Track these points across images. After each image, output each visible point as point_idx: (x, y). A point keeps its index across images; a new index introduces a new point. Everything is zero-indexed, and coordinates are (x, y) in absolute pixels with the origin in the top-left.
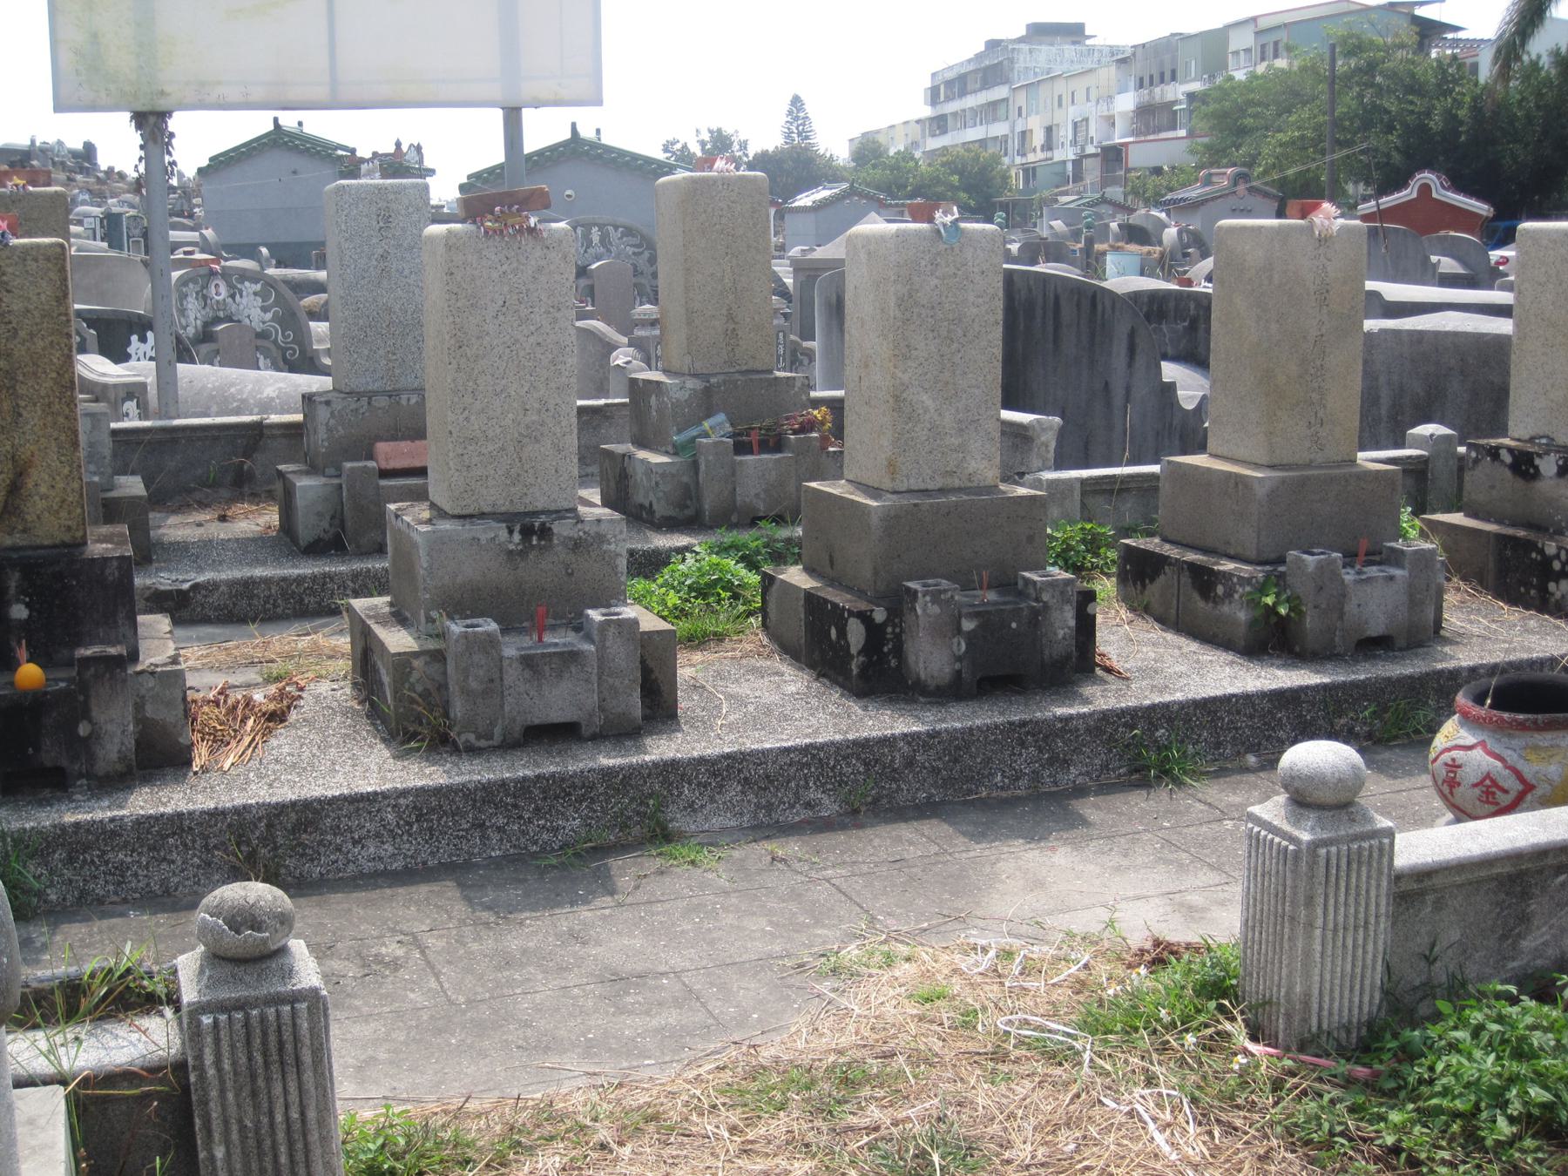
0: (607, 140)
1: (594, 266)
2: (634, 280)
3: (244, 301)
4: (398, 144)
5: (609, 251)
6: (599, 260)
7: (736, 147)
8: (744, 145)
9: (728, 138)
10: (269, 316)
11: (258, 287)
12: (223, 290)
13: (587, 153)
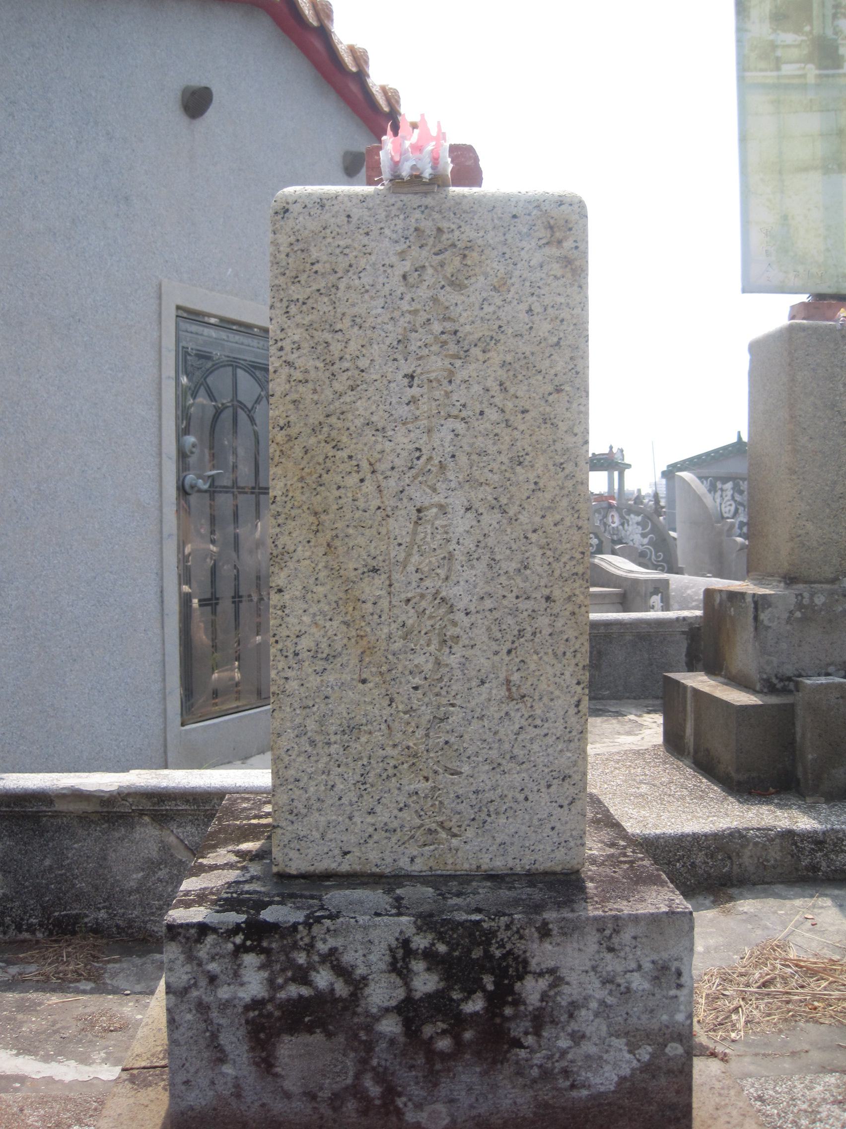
3: (630, 528)
4: (611, 448)
10: (646, 541)
11: (639, 519)
12: (617, 519)
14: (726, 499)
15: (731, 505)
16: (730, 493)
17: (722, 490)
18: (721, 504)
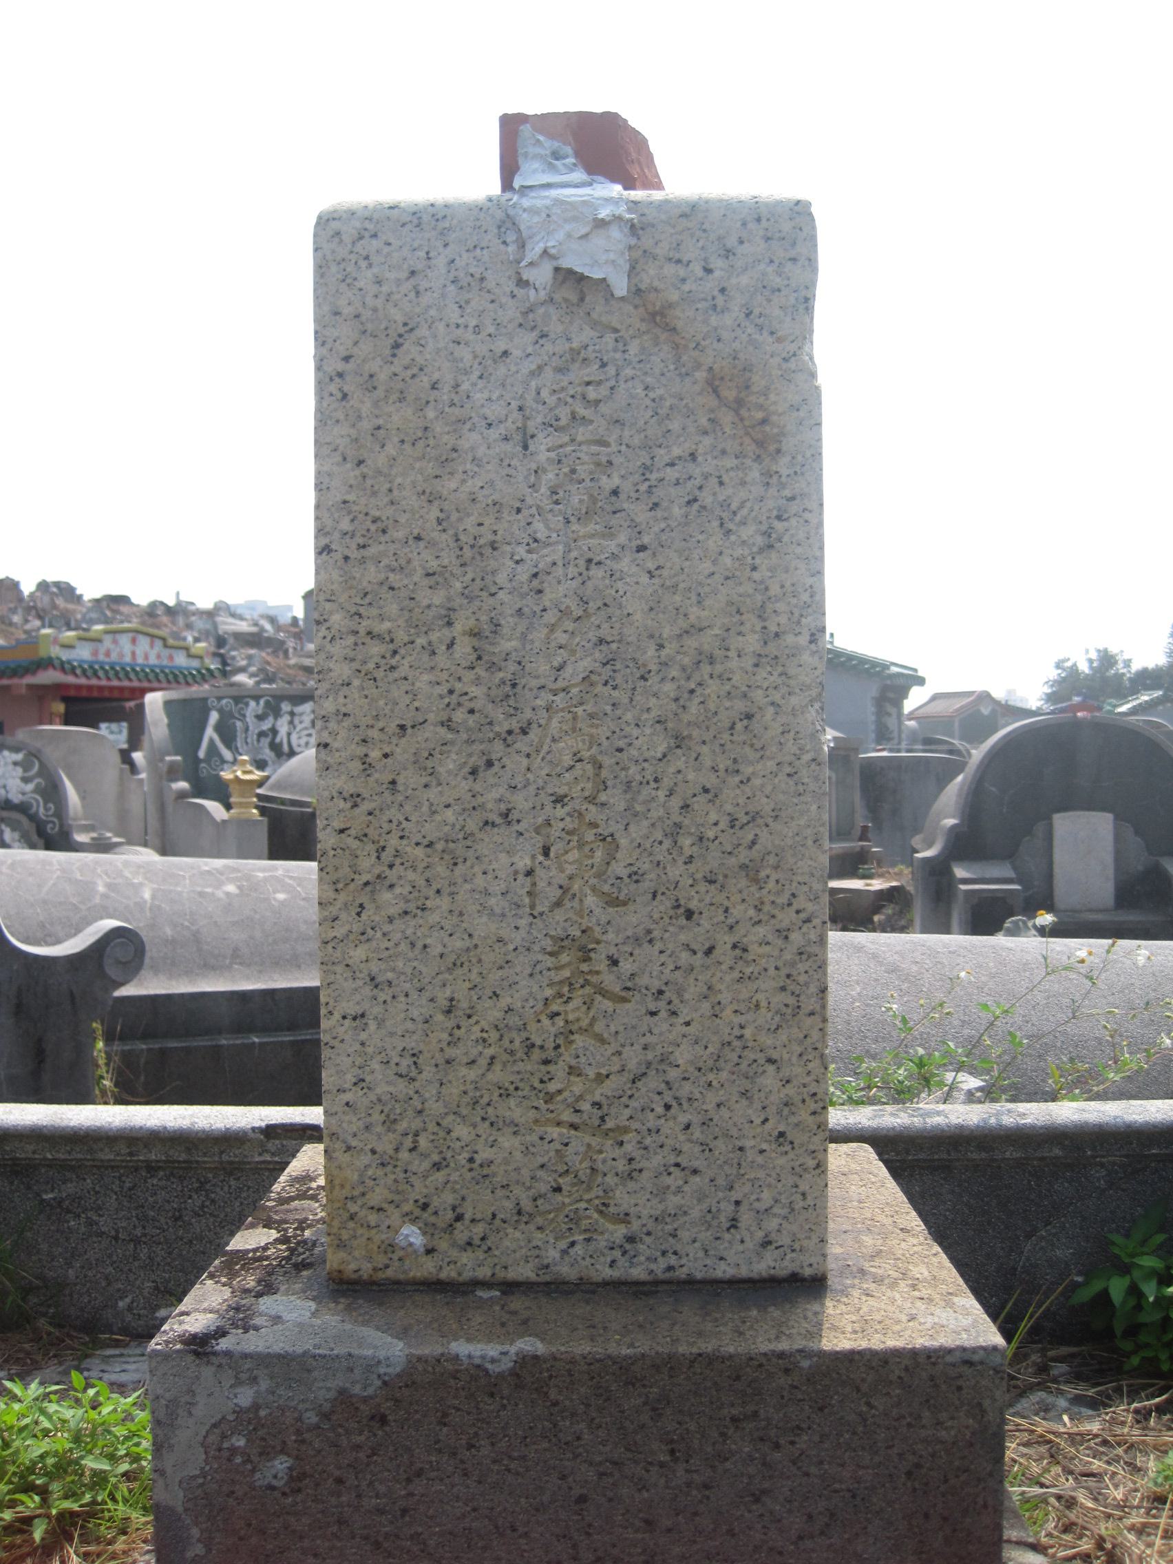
7: (1120, 665)
8: (1127, 663)
9: (1112, 657)
10: (30, 787)
11: (19, 757)
14: (299, 727)
15: (310, 735)
16: (307, 719)
17: (292, 714)
18: (289, 734)
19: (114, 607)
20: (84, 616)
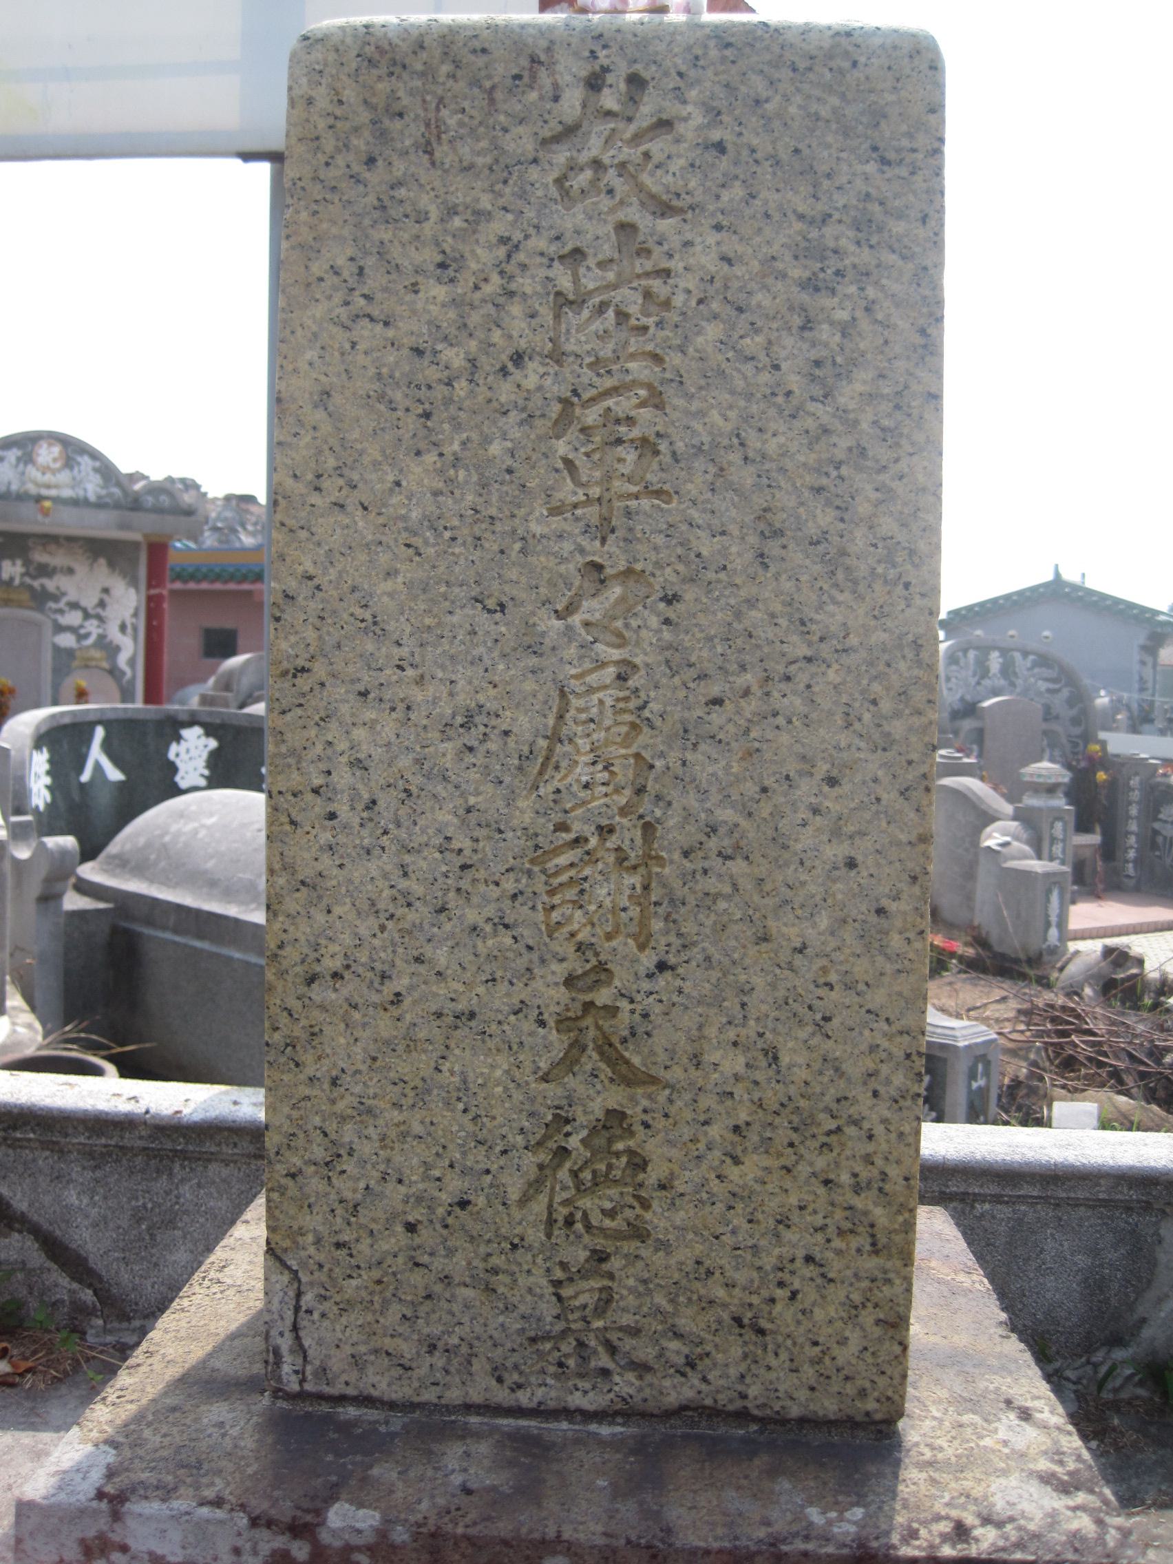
0: (1091, 584)
1: (986, 704)
2: (1045, 726)
5: (1013, 684)
6: (996, 694)
13: (1067, 595)
19: (244, 506)
20: (219, 514)
